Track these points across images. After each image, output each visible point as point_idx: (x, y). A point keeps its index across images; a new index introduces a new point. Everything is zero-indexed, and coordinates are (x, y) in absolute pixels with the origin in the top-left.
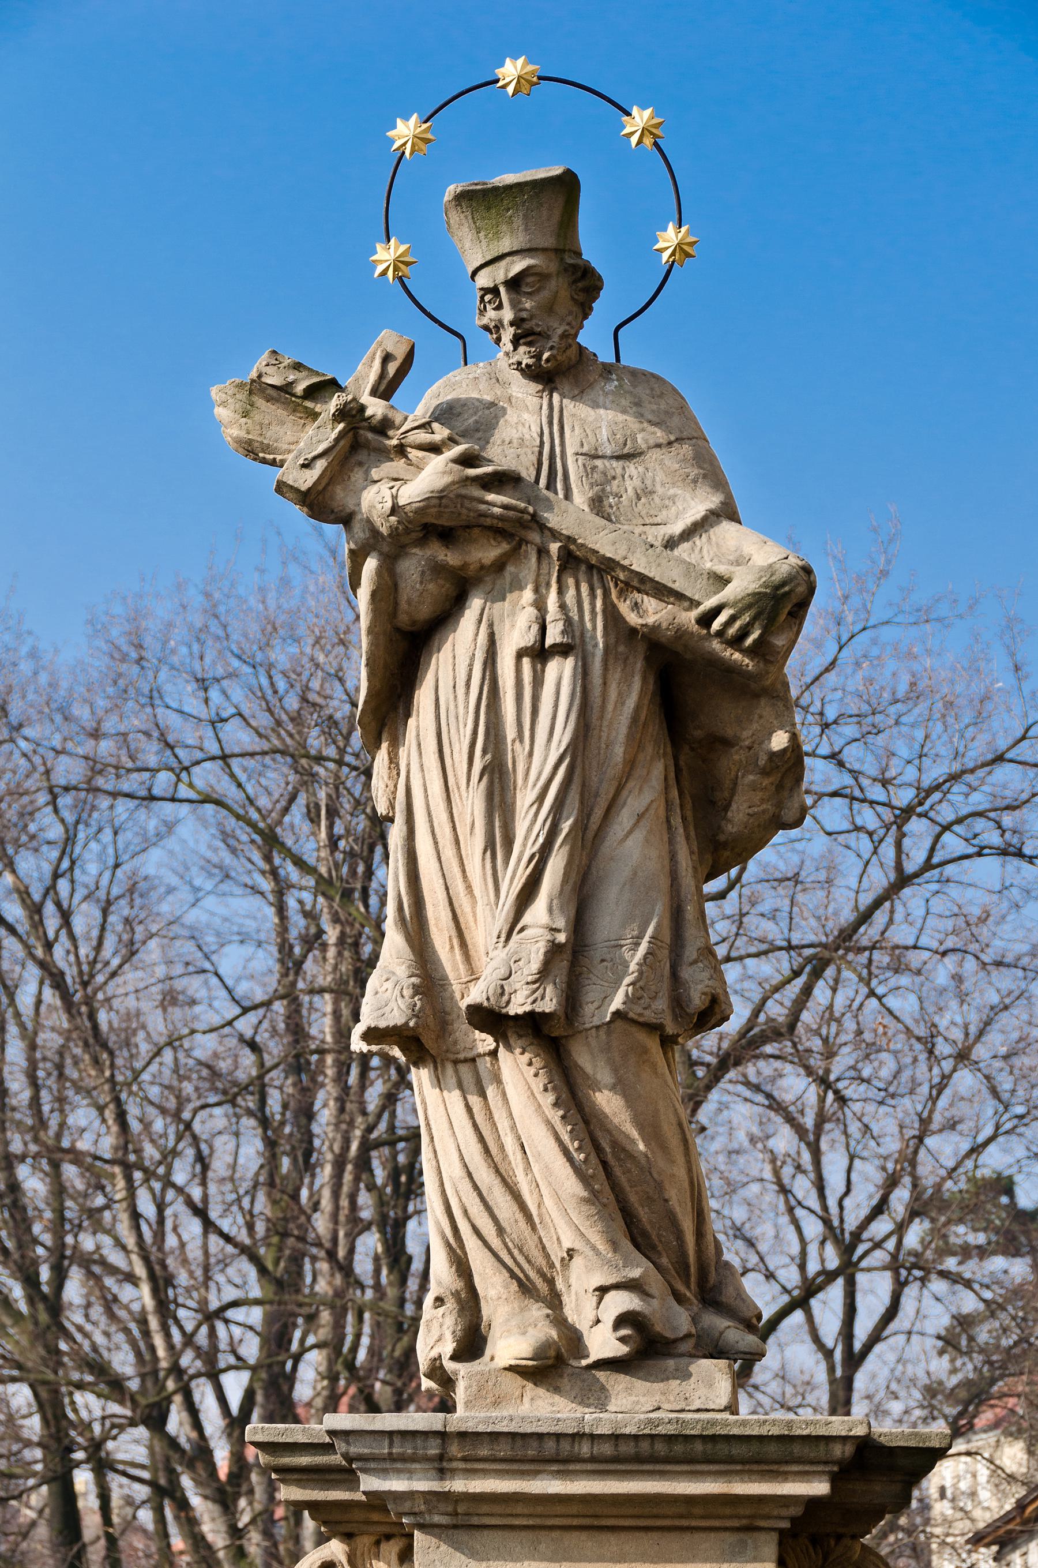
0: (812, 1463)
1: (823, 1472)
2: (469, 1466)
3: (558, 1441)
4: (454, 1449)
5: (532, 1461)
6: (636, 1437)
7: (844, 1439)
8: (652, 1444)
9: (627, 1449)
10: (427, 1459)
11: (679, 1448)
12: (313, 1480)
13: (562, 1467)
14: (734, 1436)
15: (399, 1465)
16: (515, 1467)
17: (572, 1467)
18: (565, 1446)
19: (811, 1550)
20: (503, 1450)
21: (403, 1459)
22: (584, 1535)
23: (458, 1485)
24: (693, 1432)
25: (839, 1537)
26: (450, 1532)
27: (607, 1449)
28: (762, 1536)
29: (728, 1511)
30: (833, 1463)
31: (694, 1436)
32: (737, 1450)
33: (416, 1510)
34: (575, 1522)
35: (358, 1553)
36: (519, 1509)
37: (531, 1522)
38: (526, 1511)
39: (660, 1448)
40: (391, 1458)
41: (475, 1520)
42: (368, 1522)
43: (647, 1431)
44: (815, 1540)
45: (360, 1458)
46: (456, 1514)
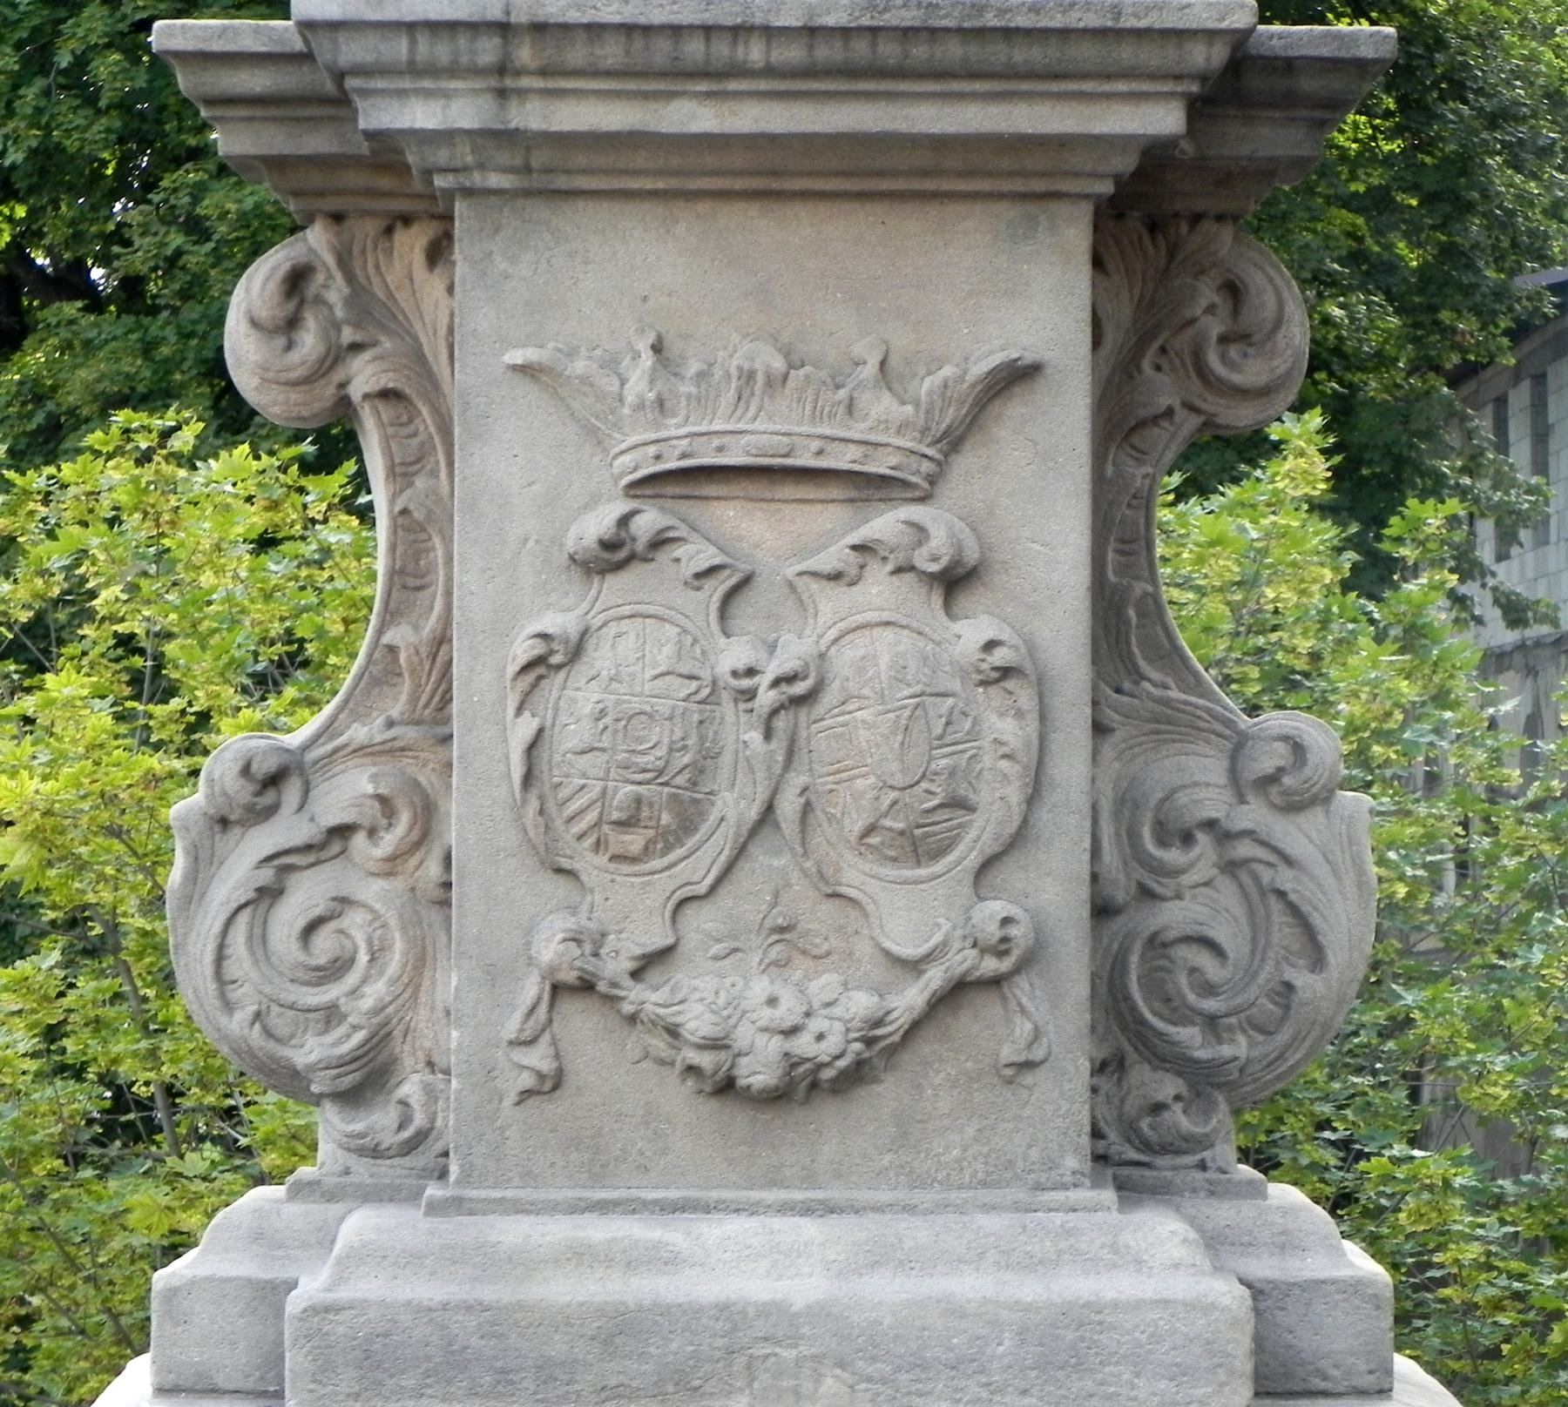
0: (1153, 76)
1: (1172, 94)
2: (552, 84)
3: (708, 40)
4: (524, 54)
5: (663, 75)
6: (845, 32)
7: (1211, 35)
8: (874, 45)
9: (827, 52)
10: (476, 71)
11: (920, 52)
12: (275, 119)
13: (714, 86)
14: (1018, 30)
15: (427, 84)
16: (632, 85)
17: (733, 85)
18: (722, 49)
19: (1147, 241)
20: (611, 53)
21: (433, 71)
22: (753, 208)
23: (532, 116)
24: (945, 23)
25: (1196, 219)
26: (520, 202)
27: (791, 54)
28: (1063, 209)
29: (1006, 163)
30: (1192, 77)
31: (947, 30)
32: (1022, 54)
33: (458, 163)
34: (739, 184)
35: (356, 250)
36: (640, 160)
37: (661, 185)
38: (651, 165)
39: (889, 51)
40: (414, 70)
41: (562, 182)
42: (371, 193)
43: (866, 21)
44: (1153, 227)
45: (360, 71)
46: (527, 170)
